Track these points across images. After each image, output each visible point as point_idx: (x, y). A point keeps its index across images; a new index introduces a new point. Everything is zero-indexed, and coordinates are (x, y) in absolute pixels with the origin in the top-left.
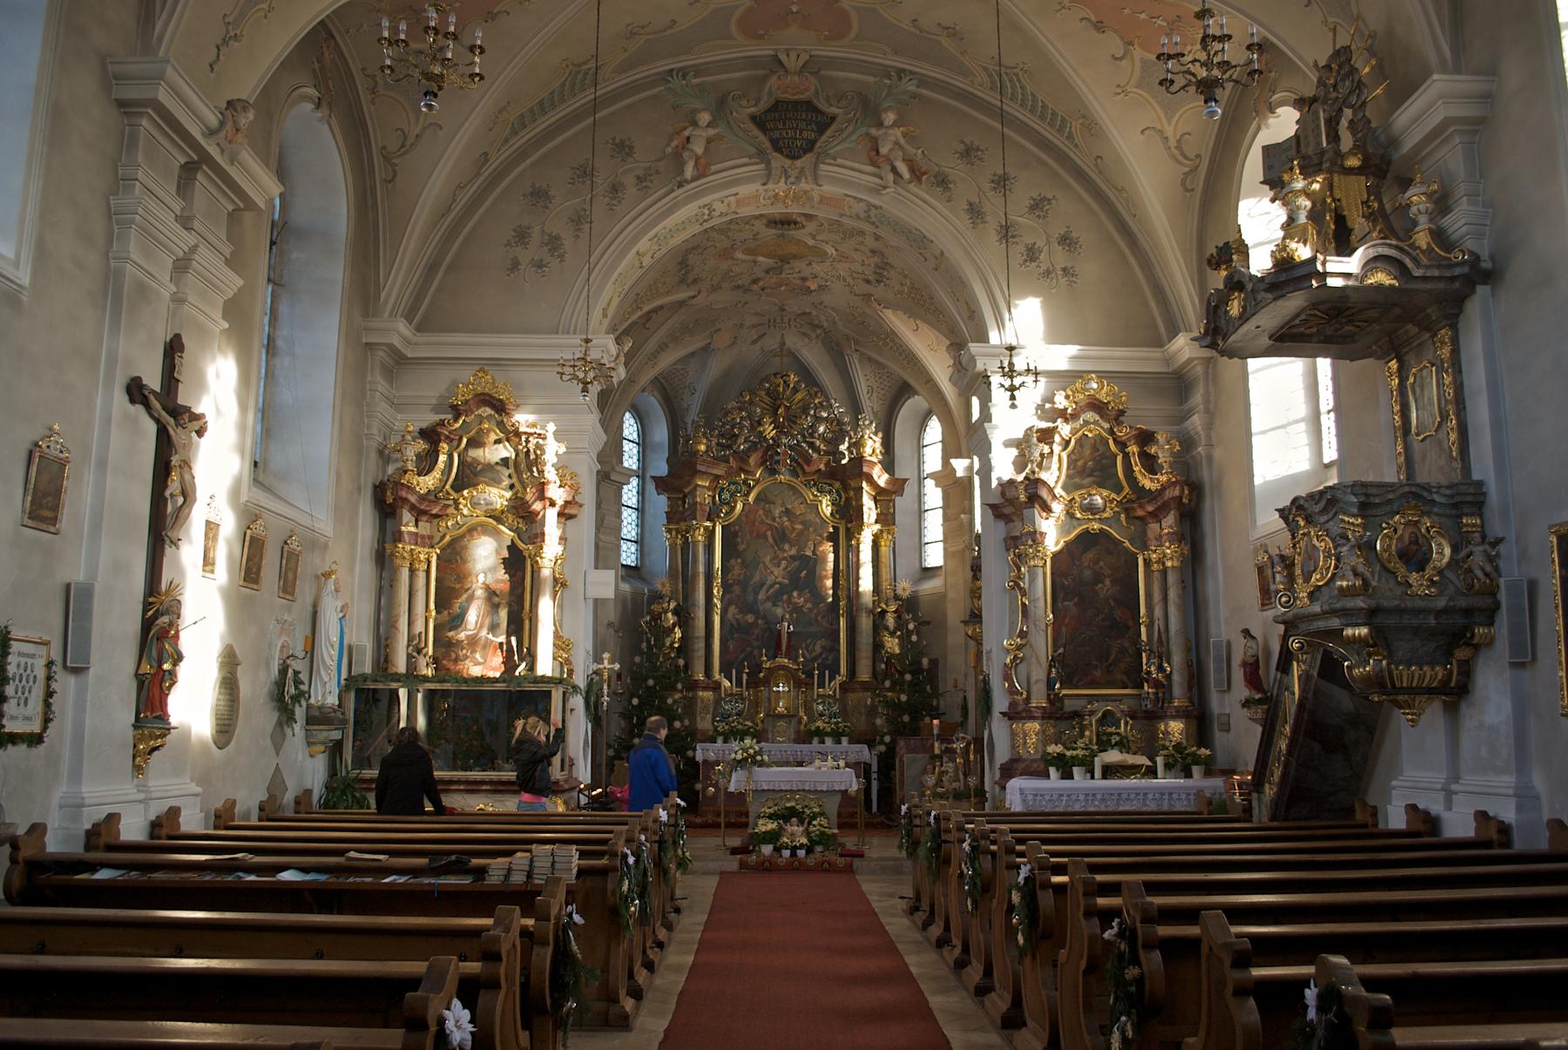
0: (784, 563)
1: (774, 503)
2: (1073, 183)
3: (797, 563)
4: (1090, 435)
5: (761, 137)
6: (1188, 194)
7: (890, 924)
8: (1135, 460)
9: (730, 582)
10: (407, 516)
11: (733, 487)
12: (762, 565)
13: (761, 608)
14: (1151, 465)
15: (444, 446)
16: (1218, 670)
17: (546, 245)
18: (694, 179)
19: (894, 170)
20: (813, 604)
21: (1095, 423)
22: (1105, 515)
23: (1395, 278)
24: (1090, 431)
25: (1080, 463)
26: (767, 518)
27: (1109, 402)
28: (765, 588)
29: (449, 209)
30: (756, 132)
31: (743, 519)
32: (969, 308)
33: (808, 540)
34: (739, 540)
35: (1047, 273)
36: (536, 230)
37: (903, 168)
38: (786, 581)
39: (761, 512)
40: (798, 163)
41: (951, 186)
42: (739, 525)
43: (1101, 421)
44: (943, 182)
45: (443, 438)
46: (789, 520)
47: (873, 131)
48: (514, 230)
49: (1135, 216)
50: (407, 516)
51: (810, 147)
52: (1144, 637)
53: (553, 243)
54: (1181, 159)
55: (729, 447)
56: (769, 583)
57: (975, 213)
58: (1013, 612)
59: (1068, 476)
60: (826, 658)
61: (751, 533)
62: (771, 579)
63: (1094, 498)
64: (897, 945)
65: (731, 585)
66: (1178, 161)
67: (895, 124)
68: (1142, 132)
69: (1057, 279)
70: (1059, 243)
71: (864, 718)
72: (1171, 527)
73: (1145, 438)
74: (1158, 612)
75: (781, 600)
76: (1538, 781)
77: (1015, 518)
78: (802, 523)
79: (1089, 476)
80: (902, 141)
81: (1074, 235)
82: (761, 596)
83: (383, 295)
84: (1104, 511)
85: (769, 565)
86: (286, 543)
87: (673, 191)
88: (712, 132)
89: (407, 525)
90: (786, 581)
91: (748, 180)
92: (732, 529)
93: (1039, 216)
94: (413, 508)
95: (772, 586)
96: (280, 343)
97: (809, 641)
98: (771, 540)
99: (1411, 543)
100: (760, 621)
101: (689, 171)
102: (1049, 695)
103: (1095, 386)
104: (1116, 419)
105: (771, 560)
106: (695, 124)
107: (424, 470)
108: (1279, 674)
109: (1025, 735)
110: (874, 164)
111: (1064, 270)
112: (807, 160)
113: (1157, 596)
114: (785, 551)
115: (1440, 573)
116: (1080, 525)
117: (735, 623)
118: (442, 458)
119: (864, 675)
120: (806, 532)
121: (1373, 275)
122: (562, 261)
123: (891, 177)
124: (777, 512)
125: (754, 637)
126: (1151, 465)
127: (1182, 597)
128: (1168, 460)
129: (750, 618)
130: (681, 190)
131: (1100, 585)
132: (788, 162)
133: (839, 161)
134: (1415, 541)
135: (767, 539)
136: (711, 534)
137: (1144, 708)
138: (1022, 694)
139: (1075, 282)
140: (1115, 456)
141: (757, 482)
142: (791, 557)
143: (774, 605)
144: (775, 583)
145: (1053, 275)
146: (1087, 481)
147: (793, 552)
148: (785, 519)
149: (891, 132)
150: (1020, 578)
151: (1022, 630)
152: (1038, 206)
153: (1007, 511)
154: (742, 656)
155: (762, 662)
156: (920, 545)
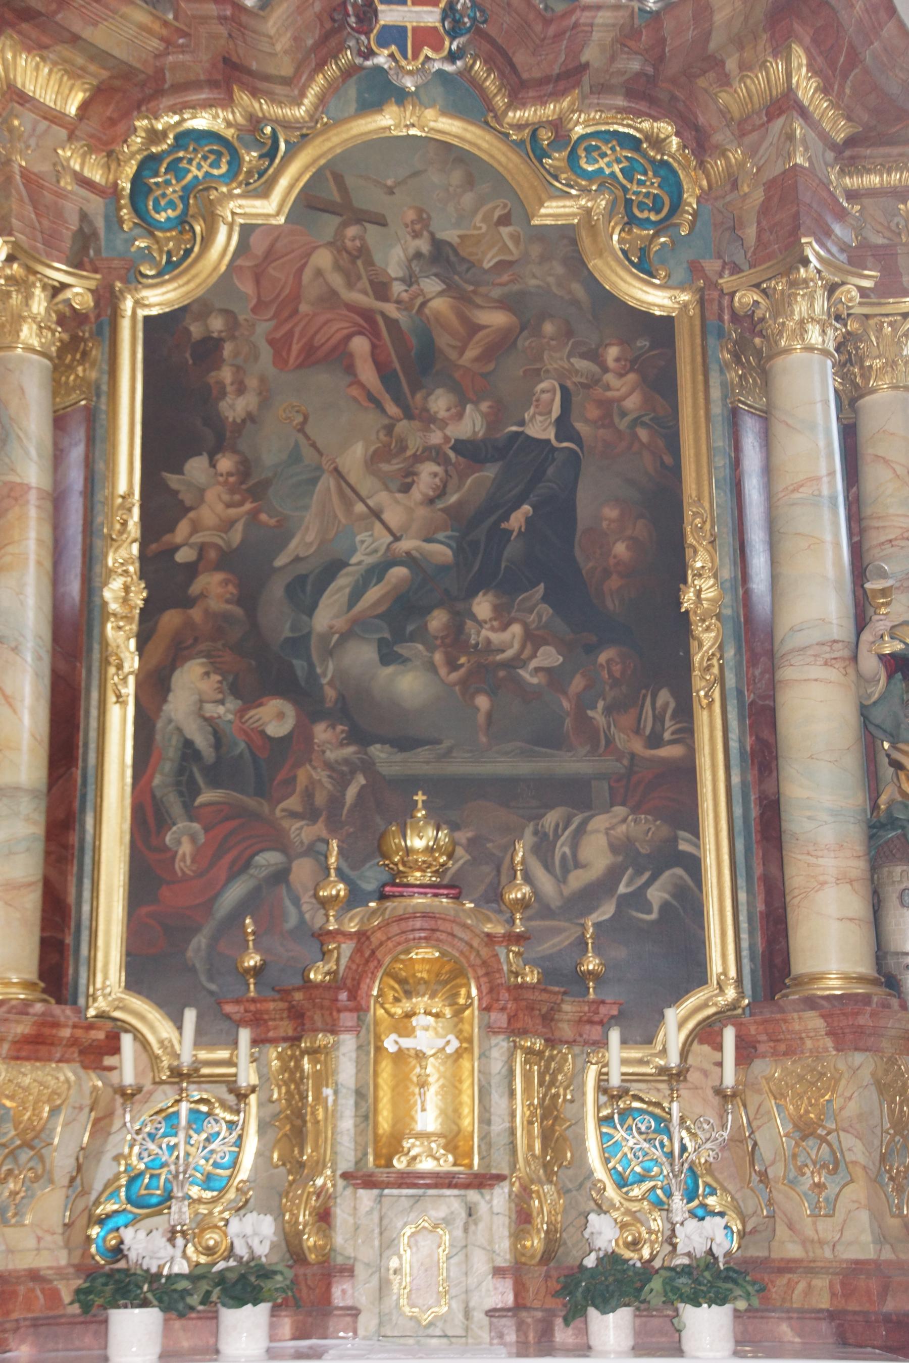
1: (381, 222)
3: (490, 472)
9: (184, 556)
12: (327, 482)
13: (327, 672)
20: (566, 647)
26: (350, 285)
28: (344, 581)
31: (247, 287)
33: (536, 375)
34: (226, 374)
39: (323, 259)
42: (228, 313)
46: (450, 289)
56: (361, 558)
60: (638, 898)
61: (279, 346)
65: (192, 570)
71: (856, 1192)
75: (421, 635)
78: (503, 304)
85: (365, 484)
92: (196, 330)
95: (377, 572)
97: (551, 818)
98: (368, 374)
100: (322, 733)
105: (373, 460)
114: (429, 420)
117: (202, 741)
120: (524, 342)
125: (293, 803)
135: (350, 369)
142: (460, 446)
143: (387, 656)
148: (431, 286)
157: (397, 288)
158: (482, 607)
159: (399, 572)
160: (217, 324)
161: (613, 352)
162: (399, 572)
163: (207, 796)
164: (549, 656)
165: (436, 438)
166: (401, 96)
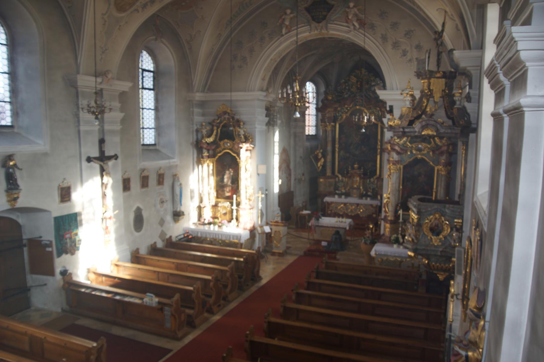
2: (422, 23)
5: (309, 16)
10: (204, 151)
15: (215, 128)
18: (286, 34)
19: (354, 25)
30: (307, 14)
35: (410, 60)
37: (356, 24)
40: (321, 24)
41: (375, 28)
44: (372, 27)
47: (347, 10)
51: (324, 18)
57: (384, 38)
67: (354, 6)
68: (437, 10)
72: (444, 160)
80: (357, 12)
83: (194, 83)
84: (424, 150)
86: (158, 172)
87: (279, 39)
88: (292, 15)
91: (305, 32)
93: (408, 38)
94: (206, 149)
96: (160, 108)
99: (435, 226)
101: (284, 31)
106: (286, 14)
107: (209, 136)
110: (347, 22)
112: (323, 24)
121: (426, 130)
123: (352, 27)
130: (283, 37)
132: (317, 24)
133: (335, 22)
149: (352, 10)
152: (408, 34)
166: (358, 106)
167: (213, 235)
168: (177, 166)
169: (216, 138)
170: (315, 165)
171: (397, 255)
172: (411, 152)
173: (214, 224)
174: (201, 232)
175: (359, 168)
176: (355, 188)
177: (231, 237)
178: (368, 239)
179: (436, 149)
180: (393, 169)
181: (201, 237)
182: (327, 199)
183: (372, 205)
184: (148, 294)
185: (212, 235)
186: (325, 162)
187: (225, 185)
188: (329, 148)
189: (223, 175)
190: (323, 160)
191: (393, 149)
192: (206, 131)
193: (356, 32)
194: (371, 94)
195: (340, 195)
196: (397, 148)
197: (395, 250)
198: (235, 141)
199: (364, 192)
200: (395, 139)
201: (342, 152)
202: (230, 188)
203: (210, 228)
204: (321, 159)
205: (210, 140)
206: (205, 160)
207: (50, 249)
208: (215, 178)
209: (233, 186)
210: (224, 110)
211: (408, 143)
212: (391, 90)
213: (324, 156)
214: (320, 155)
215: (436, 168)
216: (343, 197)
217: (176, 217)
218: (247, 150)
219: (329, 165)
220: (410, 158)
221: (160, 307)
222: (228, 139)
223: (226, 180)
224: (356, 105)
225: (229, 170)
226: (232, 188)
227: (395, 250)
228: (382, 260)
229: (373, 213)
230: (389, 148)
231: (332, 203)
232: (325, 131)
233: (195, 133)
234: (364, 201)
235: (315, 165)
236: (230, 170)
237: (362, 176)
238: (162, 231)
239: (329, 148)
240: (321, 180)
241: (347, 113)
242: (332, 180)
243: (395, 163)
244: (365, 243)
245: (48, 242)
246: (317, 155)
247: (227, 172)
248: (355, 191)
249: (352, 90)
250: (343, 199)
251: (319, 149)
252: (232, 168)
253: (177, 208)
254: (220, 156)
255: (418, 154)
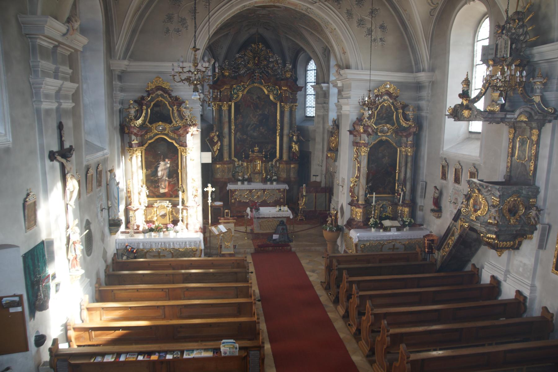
0: (257, 116)
4: (386, 105)
6: (431, 17)
7: (311, 276)
8: (400, 116)
9: (238, 123)
10: (133, 137)
11: (238, 88)
14: (406, 118)
15: (145, 107)
16: (422, 192)
17: (180, 22)
21: (387, 100)
22: (388, 134)
23: (527, 118)
24: (386, 104)
25: (381, 115)
27: (393, 93)
28: (250, 125)
29: (140, 8)
32: (343, 50)
34: (241, 108)
36: (176, 15)
38: (258, 123)
39: (249, 97)
43: (389, 99)
45: (144, 104)
48: (167, 16)
49: (409, 20)
50: (133, 137)
52: (397, 178)
53: (183, 21)
54: (431, 4)
55: (236, 72)
57: (350, 14)
58: (355, 169)
59: (376, 120)
62: (252, 122)
63: (384, 128)
64: (329, 314)
66: (430, 4)
69: (378, 43)
70: (379, 28)
72: (411, 141)
73: (405, 107)
74: (403, 169)
76: (538, 284)
77: (357, 136)
79: (384, 119)
81: (385, 25)
82: (249, 128)
83: (116, 47)
84: (388, 132)
89: (133, 141)
90: (258, 123)
98: (252, 108)
99: (513, 207)
102: (365, 199)
103: (388, 86)
104: (395, 99)
108: (453, 222)
109: (357, 212)
111: (381, 39)
113: (403, 164)
115: (520, 217)
116: (379, 137)
118: (144, 112)
119: (285, 157)
122: (187, 29)
124: (255, 97)
126: (406, 118)
127: (412, 166)
128: (412, 117)
129: (245, 137)
131: (384, 159)
134: (514, 206)
136: (230, 107)
137: (395, 202)
138: (355, 198)
139: (384, 44)
140: (394, 112)
141: (248, 86)
144: (254, 124)
145: (377, 41)
146: (384, 121)
147: (260, 112)
148: (258, 100)
150: (357, 157)
151: (357, 176)
153: (355, 133)
154: (242, 150)
155: (249, 154)
156: (305, 107)
157: (255, 100)
158: (261, 128)
159: (254, 125)
160: (240, 103)
161: (272, 106)
162: (254, 125)
163: (240, 143)
164: (266, 132)
165: (258, 113)
166: (256, 83)
167: (161, 244)
168: (108, 158)
169: (144, 121)
170: (211, 148)
171: (379, 239)
172: (377, 134)
173: (158, 230)
174: (143, 243)
175: (260, 151)
176: (257, 173)
177: (187, 243)
178: (331, 226)
179: (400, 131)
180: (364, 152)
181: (142, 250)
182: (230, 187)
183: (279, 190)
184: (224, 341)
185: (160, 244)
186: (222, 146)
187: (159, 179)
188: (226, 130)
189: (157, 168)
190: (219, 144)
191: (365, 131)
192: (135, 112)
193: (321, 3)
194: (270, 71)
195: (243, 181)
196: (370, 130)
197: (374, 234)
198: (172, 124)
199: (269, 177)
200: (366, 121)
201: (238, 134)
202: (167, 183)
203: (151, 235)
204: (217, 142)
205: (139, 122)
206: (135, 149)
207: (19, 309)
208: (145, 171)
209: (171, 180)
210: (157, 85)
211: (373, 125)
212: (356, 69)
213: (221, 137)
214: (216, 139)
215: (398, 150)
216: (246, 183)
217: (112, 228)
218: (192, 135)
219: (226, 149)
220: (375, 141)
221: (244, 354)
222: (162, 122)
223: (160, 174)
224: (254, 83)
225: (164, 161)
226: (169, 183)
227: (374, 234)
228: (365, 245)
229: (280, 198)
230: (362, 131)
231: (235, 190)
232: (220, 110)
233: (118, 113)
234: (268, 186)
235: (211, 148)
236: (167, 160)
237: (264, 159)
238: (104, 249)
239: (226, 130)
240: (218, 166)
241: (243, 91)
242: (231, 165)
243: (366, 145)
244: (331, 230)
245: (17, 299)
246: (213, 137)
247: (162, 163)
248: (256, 175)
249: (249, 65)
250: (246, 186)
251: (215, 131)
252: (168, 158)
253: (115, 216)
254: (150, 144)
255: (382, 136)
